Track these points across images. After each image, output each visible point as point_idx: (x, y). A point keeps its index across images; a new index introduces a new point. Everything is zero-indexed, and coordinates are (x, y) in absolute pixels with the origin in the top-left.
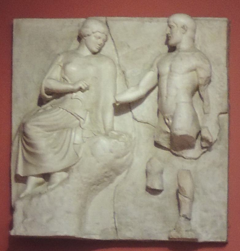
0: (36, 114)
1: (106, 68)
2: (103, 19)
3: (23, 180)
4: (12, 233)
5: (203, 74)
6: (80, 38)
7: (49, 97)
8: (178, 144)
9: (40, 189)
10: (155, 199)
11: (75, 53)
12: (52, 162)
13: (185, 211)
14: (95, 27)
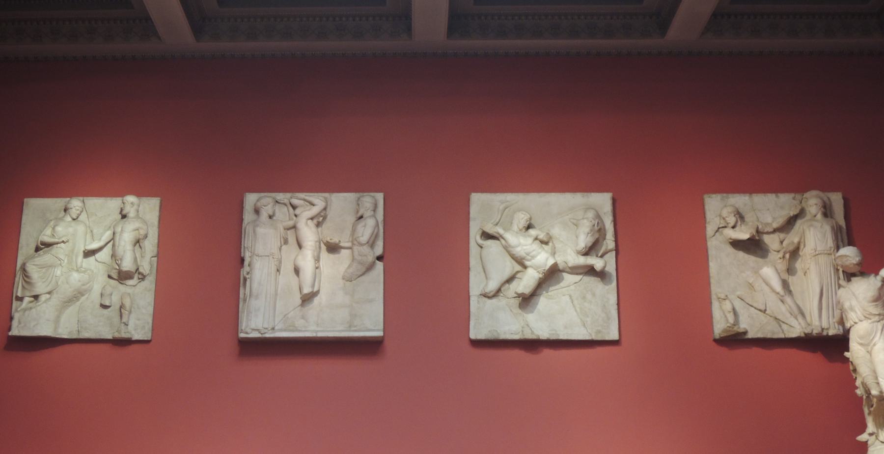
0: (33, 257)
1: (81, 229)
2: (81, 198)
3: (20, 299)
4: (10, 334)
5: (142, 232)
6: (65, 210)
7: (43, 246)
8: (123, 276)
9: (31, 305)
10: (105, 311)
11: (62, 219)
12: (40, 287)
13: (124, 320)
14: (76, 203)
